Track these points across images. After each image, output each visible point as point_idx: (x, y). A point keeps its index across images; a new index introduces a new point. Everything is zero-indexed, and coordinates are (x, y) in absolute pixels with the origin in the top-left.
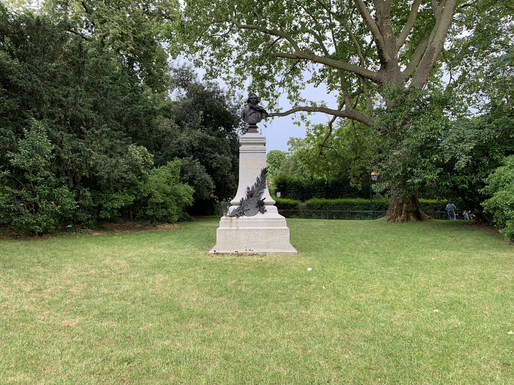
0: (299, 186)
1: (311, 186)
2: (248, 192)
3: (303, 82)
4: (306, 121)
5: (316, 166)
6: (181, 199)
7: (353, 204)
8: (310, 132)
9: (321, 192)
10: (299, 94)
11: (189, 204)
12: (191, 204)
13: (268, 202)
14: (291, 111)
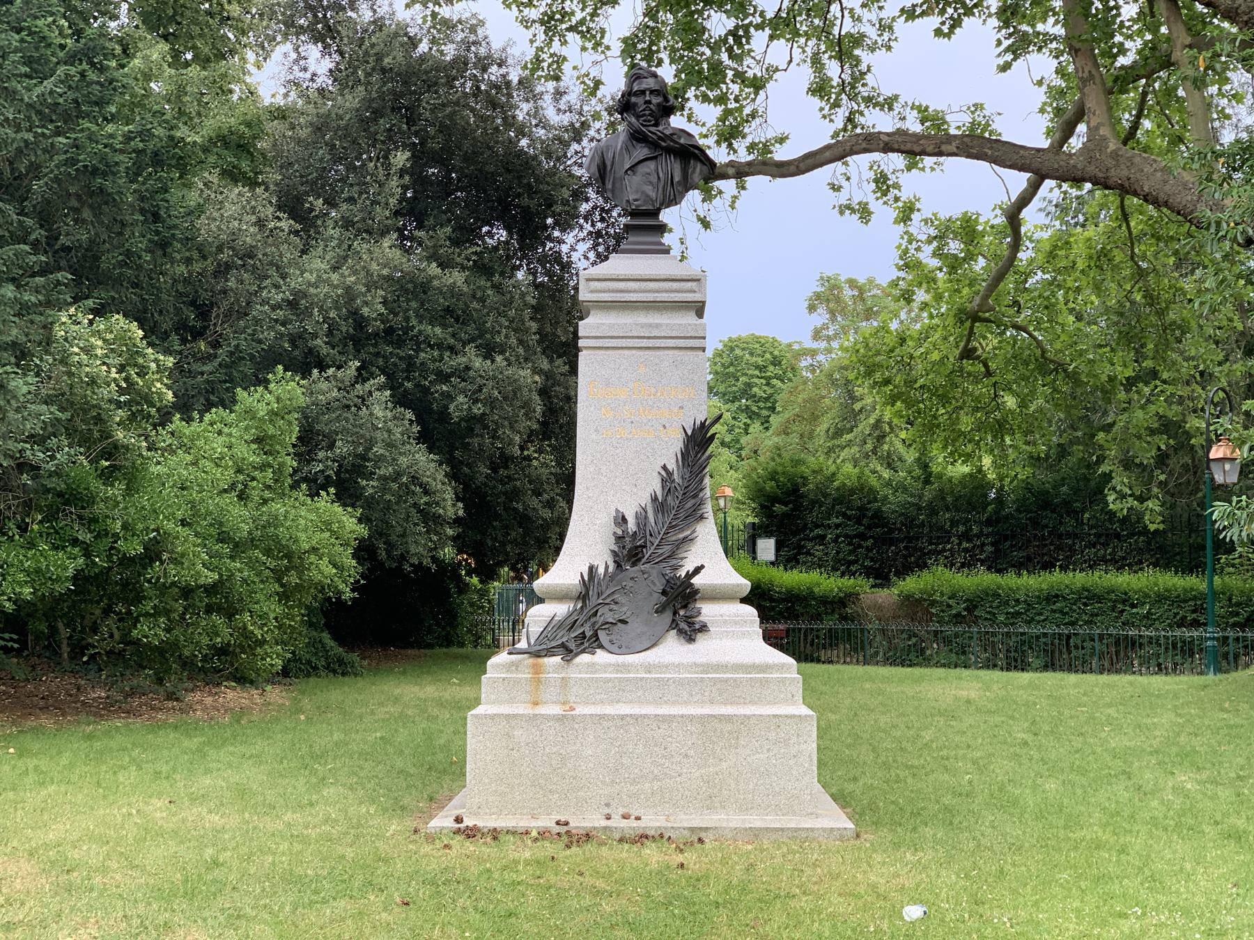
0: (862, 509)
1: (920, 509)
2: (619, 539)
3: (883, 14)
4: (897, 199)
6: (300, 570)
7: (1126, 599)
8: (918, 249)
9: (966, 536)
10: (863, 74)
11: (340, 593)
12: (348, 594)
13: (714, 588)
14: (828, 154)
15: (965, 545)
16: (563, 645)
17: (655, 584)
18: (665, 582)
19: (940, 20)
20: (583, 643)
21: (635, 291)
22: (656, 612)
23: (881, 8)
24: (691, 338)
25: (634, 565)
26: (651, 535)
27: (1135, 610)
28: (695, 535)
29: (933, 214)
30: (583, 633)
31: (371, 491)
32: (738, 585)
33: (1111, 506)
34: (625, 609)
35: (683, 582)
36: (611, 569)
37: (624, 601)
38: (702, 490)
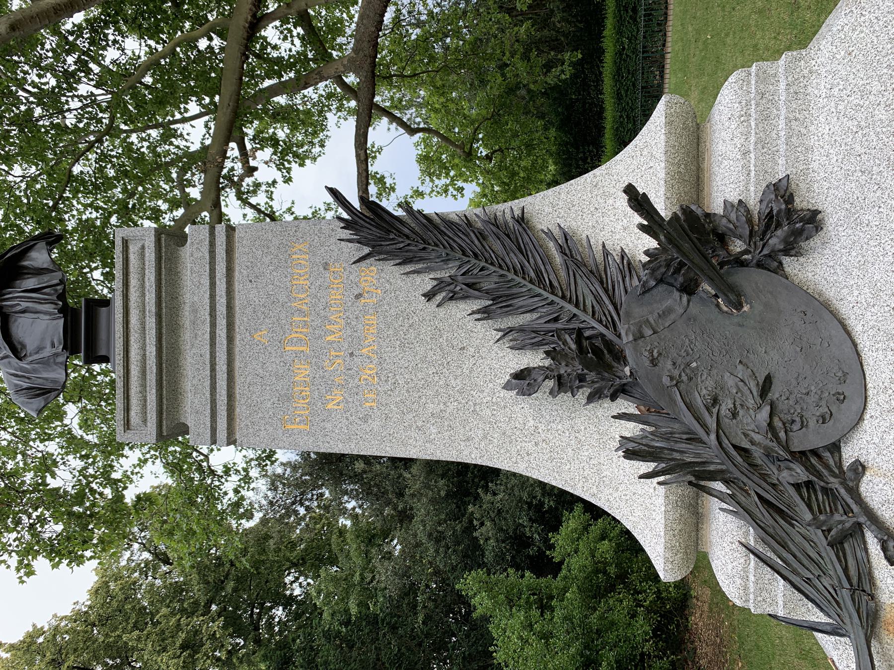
2: (562, 385)
3: (323, 208)
4: (412, 197)
5: (522, 175)
7: (619, 53)
13: (676, 177)
15: (589, 160)
16: (837, 544)
17: (669, 311)
18: (662, 288)
19: (293, 163)
20: (826, 491)
21: (143, 348)
22: (739, 306)
23: (320, 209)
25: (620, 357)
26: (556, 320)
27: (626, 47)
28: (556, 232)
30: (797, 486)
31: (551, 503)
32: (669, 123)
33: (568, 77)
34: (730, 381)
35: (670, 240)
37: (710, 383)
38: (469, 223)
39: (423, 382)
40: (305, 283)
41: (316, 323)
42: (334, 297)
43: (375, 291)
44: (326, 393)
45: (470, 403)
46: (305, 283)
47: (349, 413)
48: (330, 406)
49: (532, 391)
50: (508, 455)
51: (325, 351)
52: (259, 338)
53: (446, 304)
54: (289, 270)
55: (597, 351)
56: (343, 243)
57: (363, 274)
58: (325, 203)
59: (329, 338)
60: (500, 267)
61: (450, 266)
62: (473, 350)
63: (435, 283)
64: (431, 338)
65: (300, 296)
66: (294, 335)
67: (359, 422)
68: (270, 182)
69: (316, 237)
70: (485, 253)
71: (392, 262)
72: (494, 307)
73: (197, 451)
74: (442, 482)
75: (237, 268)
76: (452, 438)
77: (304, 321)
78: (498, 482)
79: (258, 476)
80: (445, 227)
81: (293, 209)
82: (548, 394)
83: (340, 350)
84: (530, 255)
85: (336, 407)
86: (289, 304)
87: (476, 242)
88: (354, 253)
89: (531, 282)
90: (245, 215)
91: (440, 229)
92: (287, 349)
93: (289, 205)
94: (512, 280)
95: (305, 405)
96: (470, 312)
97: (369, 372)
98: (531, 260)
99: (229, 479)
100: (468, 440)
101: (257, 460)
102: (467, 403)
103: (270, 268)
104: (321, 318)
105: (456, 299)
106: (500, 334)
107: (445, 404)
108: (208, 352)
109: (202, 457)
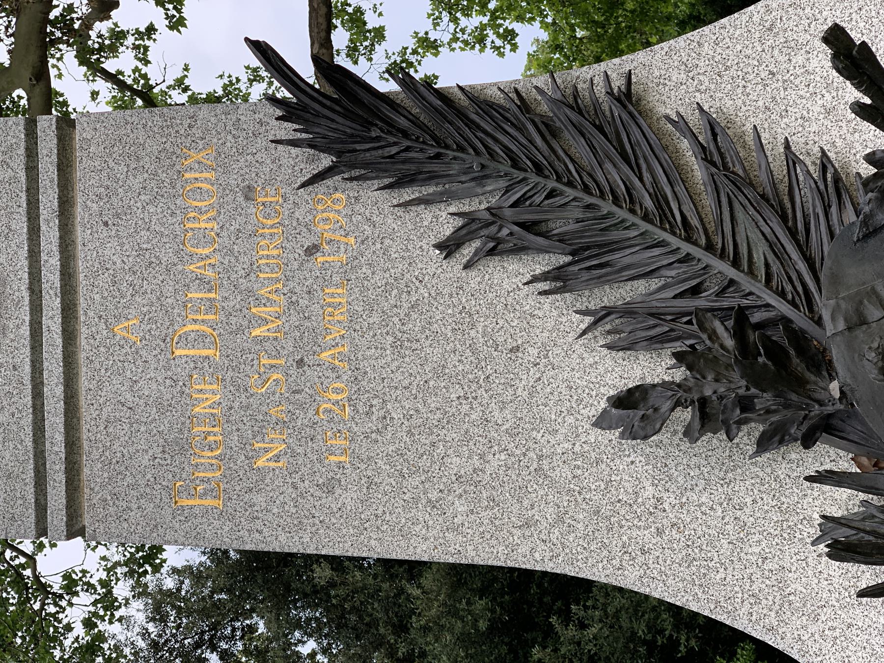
3: (244, 78)
4: (415, 52)
23: (238, 80)
24: (32, 169)
26: (695, 291)
28: (694, 119)
29: (429, 18)
31: (693, 643)
36: (845, 463)
38: (524, 105)
39: (438, 415)
40: (209, 226)
41: (232, 304)
42: (266, 252)
43: (343, 239)
44: (254, 437)
45: (531, 454)
46: (209, 226)
47: (297, 476)
48: (260, 463)
49: (649, 430)
50: (605, 553)
51: (250, 357)
52: (125, 334)
53: (483, 262)
54: (178, 202)
55: (775, 352)
56: (280, 147)
57: (320, 207)
58: (248, 68)
59: (256, 332)
60: (586, 189)
61: (489, 188)
62: (536, 352)
63: (459, 222)
64: (454, 330)
65: (200, 251)
66: (190, 327)
67: (318, 493)
68: (142, 29)
69: (229, 137)
70: (557, 163)
71: (376, 183)
72: (576, 268)
73: (14, 548)
74: (480, 604)
75: (79, 199)
76: (497, 522)
77: (210, 299)
78: (589, 603)
79: (129, 594)
80: (477, 114)
81: (187, 82)
82: (680, 435)
83: (278, 356)
84: (644, 166)
85: (272, 464)
86: (180, 267)
87: (539, 141)
88: (302, 166)
89: (646, 218)
90: (94, 95)
91: (467, 118)
92: (178, 352)
93: (179, 75)
94: (610, 215)
95: (214, 461)
96: (528, 277)
97: (334, 397)
98: (646, 176)
99: (75, 600)
100: (527, 525)
101: (126, 564)
102: (525, 455)
103: (143, 197)
104: (241, 293)
105: (501, 253)
106: (588, 320)
107: (482, 456)
108: (28, 360)
109: (23, 560)
